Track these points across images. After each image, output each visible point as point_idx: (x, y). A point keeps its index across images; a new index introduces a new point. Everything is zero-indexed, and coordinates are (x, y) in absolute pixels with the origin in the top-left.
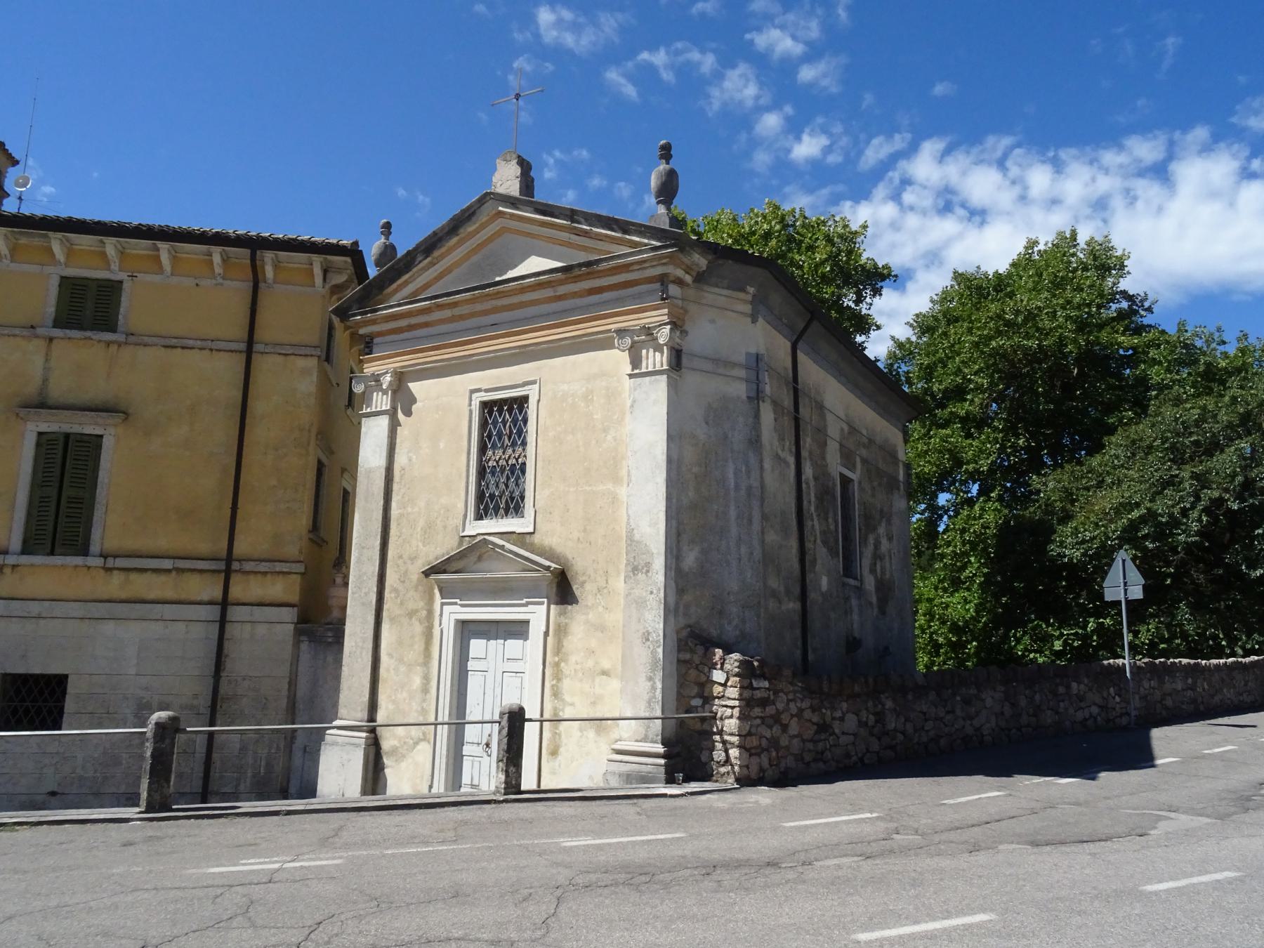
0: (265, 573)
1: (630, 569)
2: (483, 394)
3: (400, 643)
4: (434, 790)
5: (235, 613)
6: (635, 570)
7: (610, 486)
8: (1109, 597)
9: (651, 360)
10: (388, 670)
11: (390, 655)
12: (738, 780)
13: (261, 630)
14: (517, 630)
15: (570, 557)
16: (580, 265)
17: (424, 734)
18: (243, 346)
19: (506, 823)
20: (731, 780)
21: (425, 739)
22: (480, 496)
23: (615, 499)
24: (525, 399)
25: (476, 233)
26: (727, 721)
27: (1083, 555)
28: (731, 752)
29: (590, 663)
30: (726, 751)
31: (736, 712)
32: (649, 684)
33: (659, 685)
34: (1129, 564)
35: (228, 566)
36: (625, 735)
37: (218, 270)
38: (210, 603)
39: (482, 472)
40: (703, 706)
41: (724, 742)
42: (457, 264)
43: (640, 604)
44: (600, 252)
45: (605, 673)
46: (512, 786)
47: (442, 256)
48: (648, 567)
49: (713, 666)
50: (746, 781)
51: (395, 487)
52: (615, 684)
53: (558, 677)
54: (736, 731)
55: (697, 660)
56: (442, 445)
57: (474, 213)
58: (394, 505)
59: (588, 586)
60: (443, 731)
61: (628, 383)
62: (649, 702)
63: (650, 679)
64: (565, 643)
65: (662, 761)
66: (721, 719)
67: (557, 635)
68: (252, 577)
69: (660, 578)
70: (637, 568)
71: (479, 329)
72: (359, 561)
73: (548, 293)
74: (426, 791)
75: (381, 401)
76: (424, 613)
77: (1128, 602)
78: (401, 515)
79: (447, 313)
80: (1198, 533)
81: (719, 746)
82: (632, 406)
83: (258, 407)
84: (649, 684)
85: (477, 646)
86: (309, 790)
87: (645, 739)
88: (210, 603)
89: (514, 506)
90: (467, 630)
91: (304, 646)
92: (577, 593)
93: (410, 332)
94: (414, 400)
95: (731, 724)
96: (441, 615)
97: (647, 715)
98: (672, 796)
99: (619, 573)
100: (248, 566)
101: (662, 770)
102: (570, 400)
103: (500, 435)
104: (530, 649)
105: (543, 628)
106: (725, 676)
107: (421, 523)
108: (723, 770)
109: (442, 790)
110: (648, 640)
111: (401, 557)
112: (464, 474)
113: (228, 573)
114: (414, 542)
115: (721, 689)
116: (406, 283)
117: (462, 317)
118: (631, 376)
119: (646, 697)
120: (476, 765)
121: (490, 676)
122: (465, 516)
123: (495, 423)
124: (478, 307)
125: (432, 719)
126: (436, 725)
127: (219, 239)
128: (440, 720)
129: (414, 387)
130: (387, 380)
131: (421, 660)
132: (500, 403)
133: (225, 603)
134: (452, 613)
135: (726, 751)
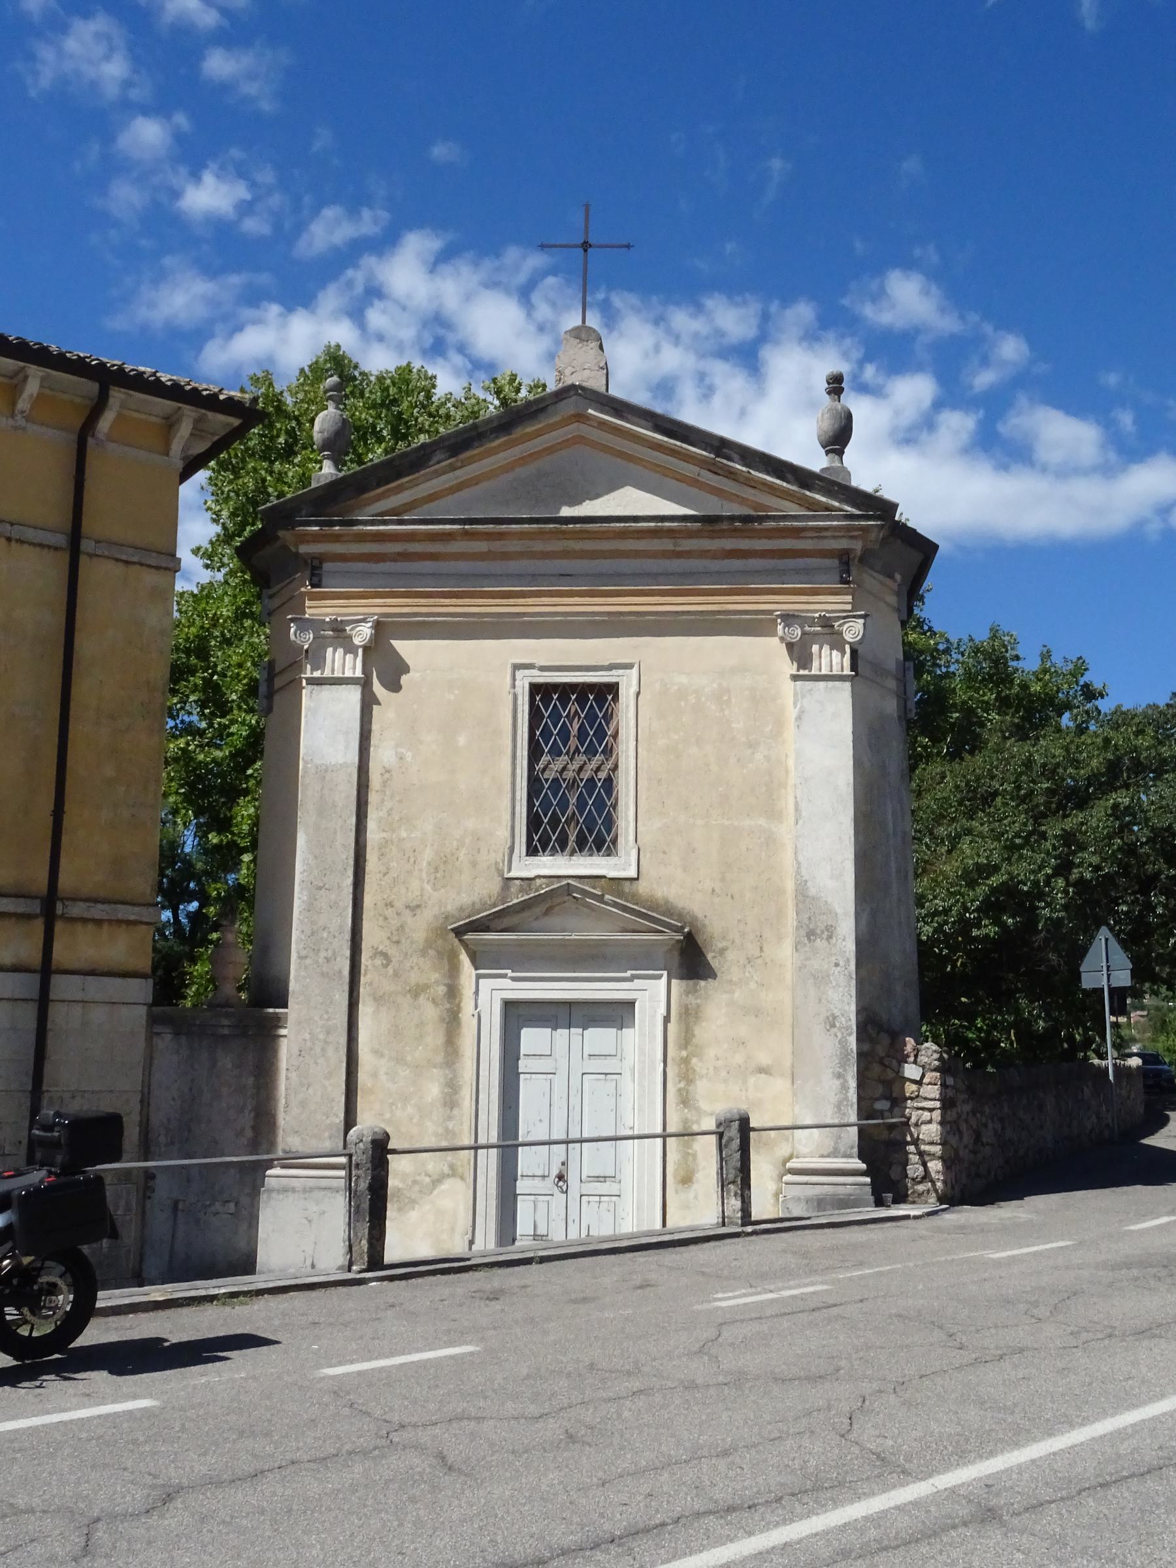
0: (98, 922)
1: (803, 932)
2: (535, 672)
3: (396, 1032)
4: (478, 1246)
5: (62, 986)
6: (811, 934)
7: (762, 822)
8: (1087, 982)
9: (825, 661)
10: (375, 1075)
11: (378, 1053)
12: (941, 1200)
13: (98, 1015)
14: (617, 1014)
15: (700, 915)
16: (732, 518)
17: (452, 1167)
18: (61, 540)
19: (983, 1229)
20: (933, 1199)
21: (454, 1172)
22: (534, 822)
23: (770, 841)
24: (612, 689)
25: (534, 439)
26: (924, 1128)
27: (935, 931)
28: (929, 1164)
29: (739, 1058)
30: (924, 1164)
31: (937, 1115)
32: (837, 1083)
33: (853, 1084)
34: (1113, 942)
35: (49, 907)
36: (804, 1150)
37: (23, 404)
38: (16, 969)
39: (534, 783)
40: (891, 1110)
41: (921, 1154)
42: (491, 475)
43: (820, 979)
44: (743, 501)
45: (762, 1070)
46: (375, 1261)
47: (471, 460)
48: (830, 933)
49: (904, 1059)
50: (953, 1198)
51: (373, 798)
52: (780, 1085)
53: (688, 1076)
54: (937, 1139)
55: (881, 1051)
56: (462, 740)
57: (543, 410)
58: (371, 825)
59: (731, 955)
60: (489, 1161)
61: (789, 687)
62: (839, 1106)
63: (839, 1076)
64: (697, 1031)
65: (868, 1180)
66: (917, 1125)
67: (684, 1023)
68: (79, 927)
69: (850, 947)
70: (812, 933)
71: (534, 578)
72: (309, 908)
73: (667, 545)
74: (658, 1225)
75: (344, 663)
76: (441, 990)
77: (1112, 991)
78: (385, 843)
79: (482, 546)
80: (1065, 907)
81: (914, 1158)
82: (799, 718)
83: (85, 646)
84: (837, 1083)
85: (532, 1038)
86: (246, 1265)
87: (834, 1153)
88: (16, 969)
89: (598, 836)
90: (517, 1015)
91: (165, 1041)
92: (714, 963)
93: (399, 563)
94: (405, 669)
95: (930, 1131)
96: (477, 992)
97: (836, 1121)
98: (916, 1217)
99: (780, 938)
100: (77, 910)
101: (869, 1189)
102: (692, 699)
103: (565, 734)
104: (641, 1042)
105: (662, 1011)
106: (921, 1069)
107: (428, 854)
108: (920, 1188)
109: (491, 1245)
110: (833, 1026)
111: (390, 905)
112: (508, 787)
113: (50, 917)
114: (415, 884)
115: (914, 1087)
116: (400, 489)
117: (505, 556)
118: (795, 678)
119: (834, 1099)
120: (542, 1207)
121: (559, 1082)
122: (512, 849)
123: (555, 716)
124: (538, 546)
125: (467, 1140)
126: (567, 1142)
127: (41, 356)
128: (482, 1140)
129: (404, 647)
130: (363, 633)
131: (439, 1058)
132: (565, 690)
133: (46, 970)
134: (487, 994)
135: (924, 1164)
